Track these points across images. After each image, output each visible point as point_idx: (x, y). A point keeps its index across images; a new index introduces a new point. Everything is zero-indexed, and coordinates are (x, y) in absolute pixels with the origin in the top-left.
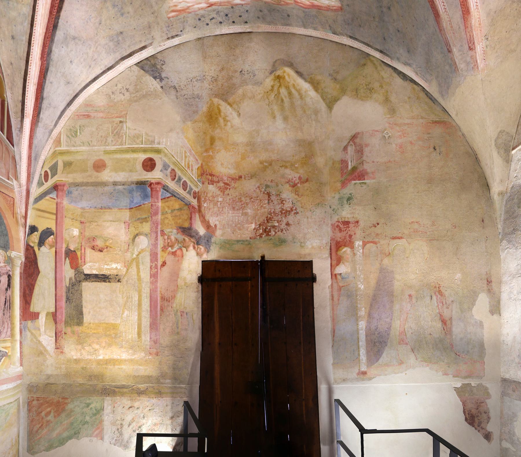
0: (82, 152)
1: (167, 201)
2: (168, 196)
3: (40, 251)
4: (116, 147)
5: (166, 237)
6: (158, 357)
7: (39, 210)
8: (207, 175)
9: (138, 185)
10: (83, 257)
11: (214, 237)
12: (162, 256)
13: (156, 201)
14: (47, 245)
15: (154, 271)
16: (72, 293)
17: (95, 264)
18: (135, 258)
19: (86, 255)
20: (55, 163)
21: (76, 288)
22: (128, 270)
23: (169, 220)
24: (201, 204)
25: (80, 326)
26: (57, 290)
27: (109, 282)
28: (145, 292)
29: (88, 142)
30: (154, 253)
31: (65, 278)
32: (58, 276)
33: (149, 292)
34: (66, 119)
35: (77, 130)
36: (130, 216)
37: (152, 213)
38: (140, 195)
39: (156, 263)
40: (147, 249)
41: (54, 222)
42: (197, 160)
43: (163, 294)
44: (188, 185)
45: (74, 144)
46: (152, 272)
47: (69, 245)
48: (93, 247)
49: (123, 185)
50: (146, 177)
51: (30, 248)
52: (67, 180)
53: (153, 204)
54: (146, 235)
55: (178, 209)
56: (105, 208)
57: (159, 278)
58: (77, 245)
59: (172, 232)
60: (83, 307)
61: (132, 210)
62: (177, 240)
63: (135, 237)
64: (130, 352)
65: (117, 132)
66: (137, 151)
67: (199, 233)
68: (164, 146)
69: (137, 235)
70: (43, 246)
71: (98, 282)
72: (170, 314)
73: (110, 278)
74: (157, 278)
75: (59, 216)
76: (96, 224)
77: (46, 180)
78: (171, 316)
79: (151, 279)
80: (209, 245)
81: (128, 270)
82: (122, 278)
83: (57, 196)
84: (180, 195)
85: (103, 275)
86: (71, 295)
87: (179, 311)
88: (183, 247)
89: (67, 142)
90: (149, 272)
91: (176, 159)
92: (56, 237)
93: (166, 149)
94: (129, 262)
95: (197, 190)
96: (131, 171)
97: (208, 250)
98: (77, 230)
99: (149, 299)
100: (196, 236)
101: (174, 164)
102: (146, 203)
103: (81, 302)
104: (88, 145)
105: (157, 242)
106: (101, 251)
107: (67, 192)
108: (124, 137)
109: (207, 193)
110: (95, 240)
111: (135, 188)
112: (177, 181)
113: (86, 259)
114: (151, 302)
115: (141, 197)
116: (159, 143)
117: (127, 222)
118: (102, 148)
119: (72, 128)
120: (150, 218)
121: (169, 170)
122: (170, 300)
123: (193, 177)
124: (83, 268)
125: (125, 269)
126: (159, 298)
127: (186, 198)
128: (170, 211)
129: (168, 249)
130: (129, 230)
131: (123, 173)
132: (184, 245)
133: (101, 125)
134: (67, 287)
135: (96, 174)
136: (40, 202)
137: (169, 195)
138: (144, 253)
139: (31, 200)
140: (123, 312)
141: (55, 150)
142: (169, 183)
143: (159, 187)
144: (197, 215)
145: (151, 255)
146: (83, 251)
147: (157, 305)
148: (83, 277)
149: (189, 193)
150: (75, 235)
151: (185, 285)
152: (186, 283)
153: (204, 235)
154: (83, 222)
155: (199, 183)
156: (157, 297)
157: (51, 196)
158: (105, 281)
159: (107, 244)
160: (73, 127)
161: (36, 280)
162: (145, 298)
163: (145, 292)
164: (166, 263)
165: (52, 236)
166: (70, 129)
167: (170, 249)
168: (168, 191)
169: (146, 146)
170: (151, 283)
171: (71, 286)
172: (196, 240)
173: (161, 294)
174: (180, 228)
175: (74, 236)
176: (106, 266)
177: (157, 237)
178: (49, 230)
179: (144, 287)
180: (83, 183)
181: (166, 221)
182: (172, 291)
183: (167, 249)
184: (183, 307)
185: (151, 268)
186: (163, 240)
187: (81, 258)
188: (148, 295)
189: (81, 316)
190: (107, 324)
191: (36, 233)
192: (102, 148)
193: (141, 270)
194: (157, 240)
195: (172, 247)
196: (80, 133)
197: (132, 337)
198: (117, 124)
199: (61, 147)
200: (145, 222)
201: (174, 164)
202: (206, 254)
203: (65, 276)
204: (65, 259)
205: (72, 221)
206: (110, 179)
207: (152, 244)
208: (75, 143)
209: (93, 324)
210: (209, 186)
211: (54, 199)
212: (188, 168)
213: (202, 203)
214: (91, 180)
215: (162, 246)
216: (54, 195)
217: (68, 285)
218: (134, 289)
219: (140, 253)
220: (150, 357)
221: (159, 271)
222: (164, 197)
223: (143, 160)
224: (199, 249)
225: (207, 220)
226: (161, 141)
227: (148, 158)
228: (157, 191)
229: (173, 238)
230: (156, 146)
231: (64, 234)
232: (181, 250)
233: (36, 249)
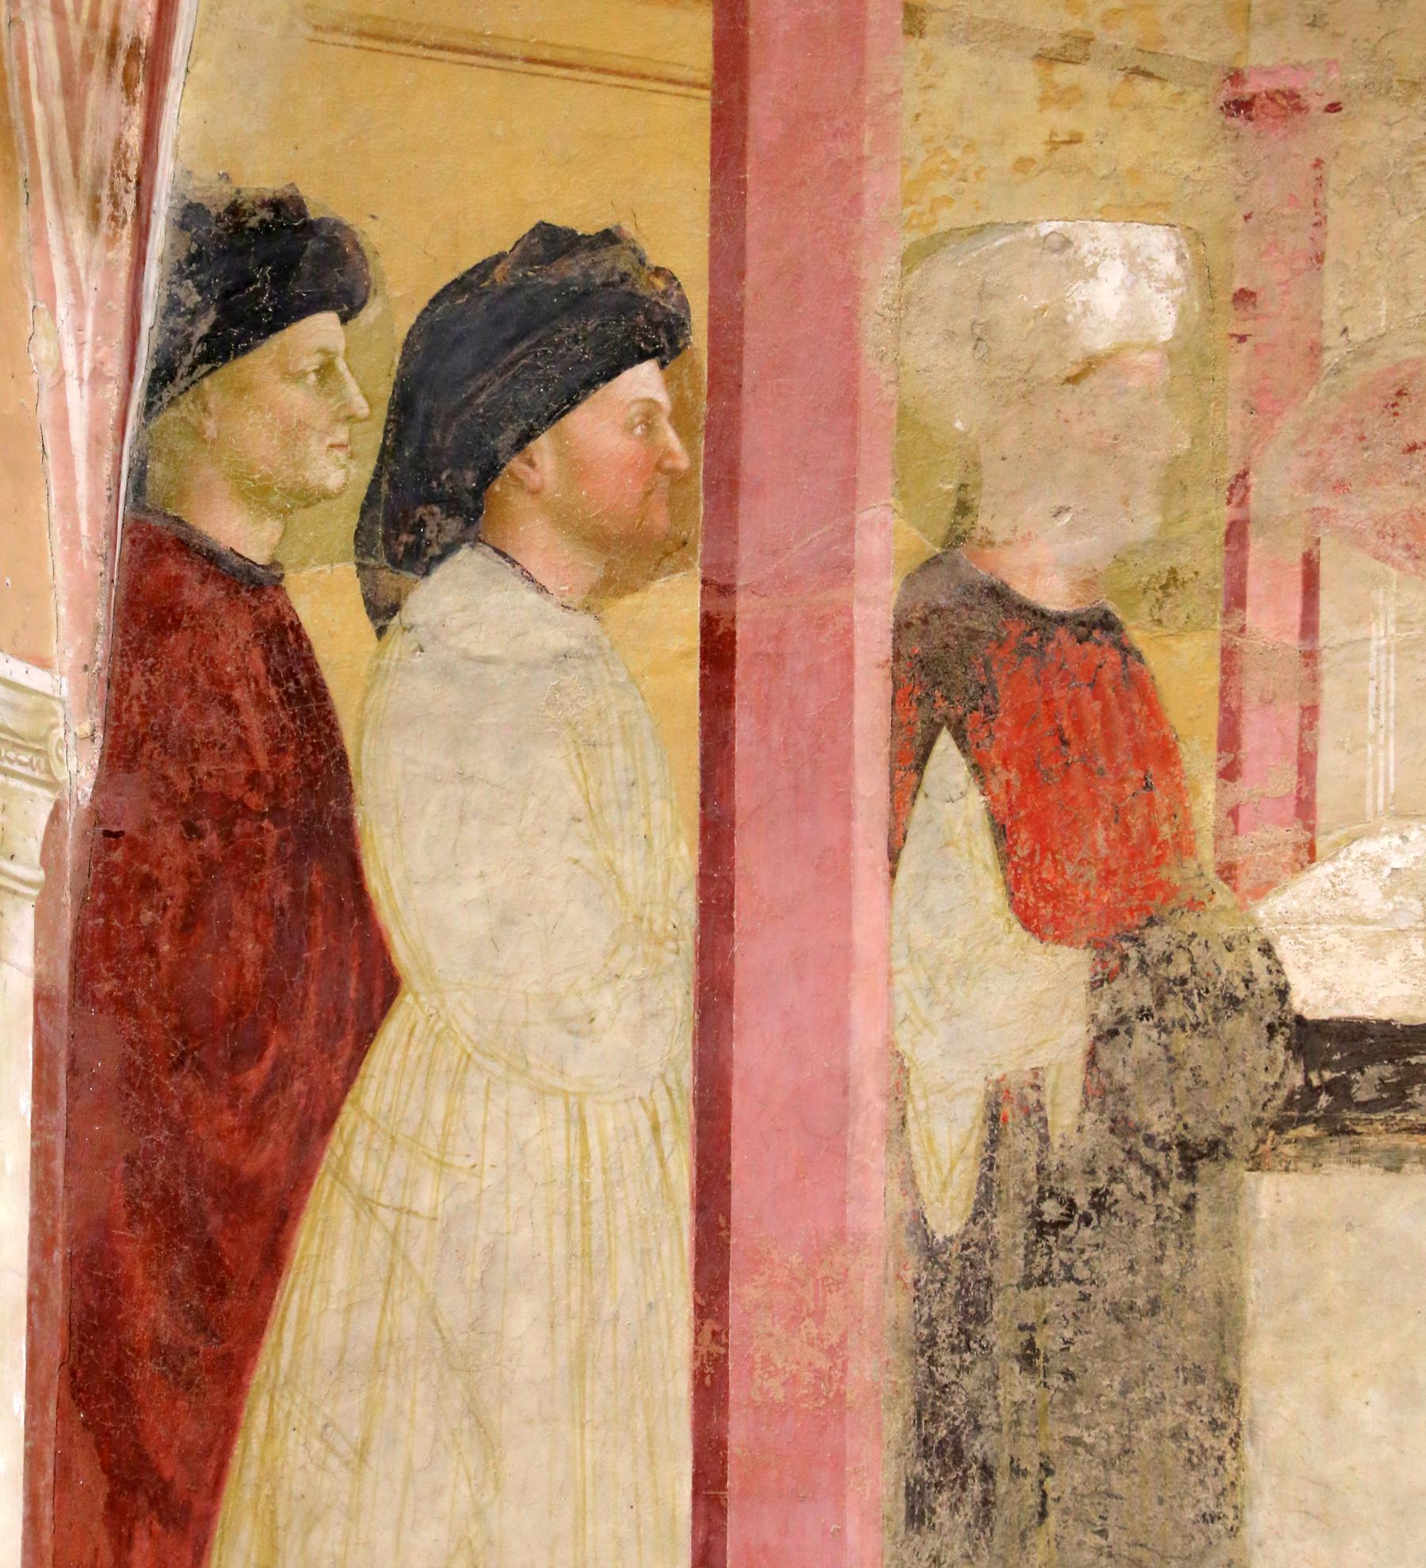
19: (1332, 693)
31: (898, 1093)
113: (1328, 761)
124: (1268, 911)
134: (931, 1252)
187: (1229, 737)
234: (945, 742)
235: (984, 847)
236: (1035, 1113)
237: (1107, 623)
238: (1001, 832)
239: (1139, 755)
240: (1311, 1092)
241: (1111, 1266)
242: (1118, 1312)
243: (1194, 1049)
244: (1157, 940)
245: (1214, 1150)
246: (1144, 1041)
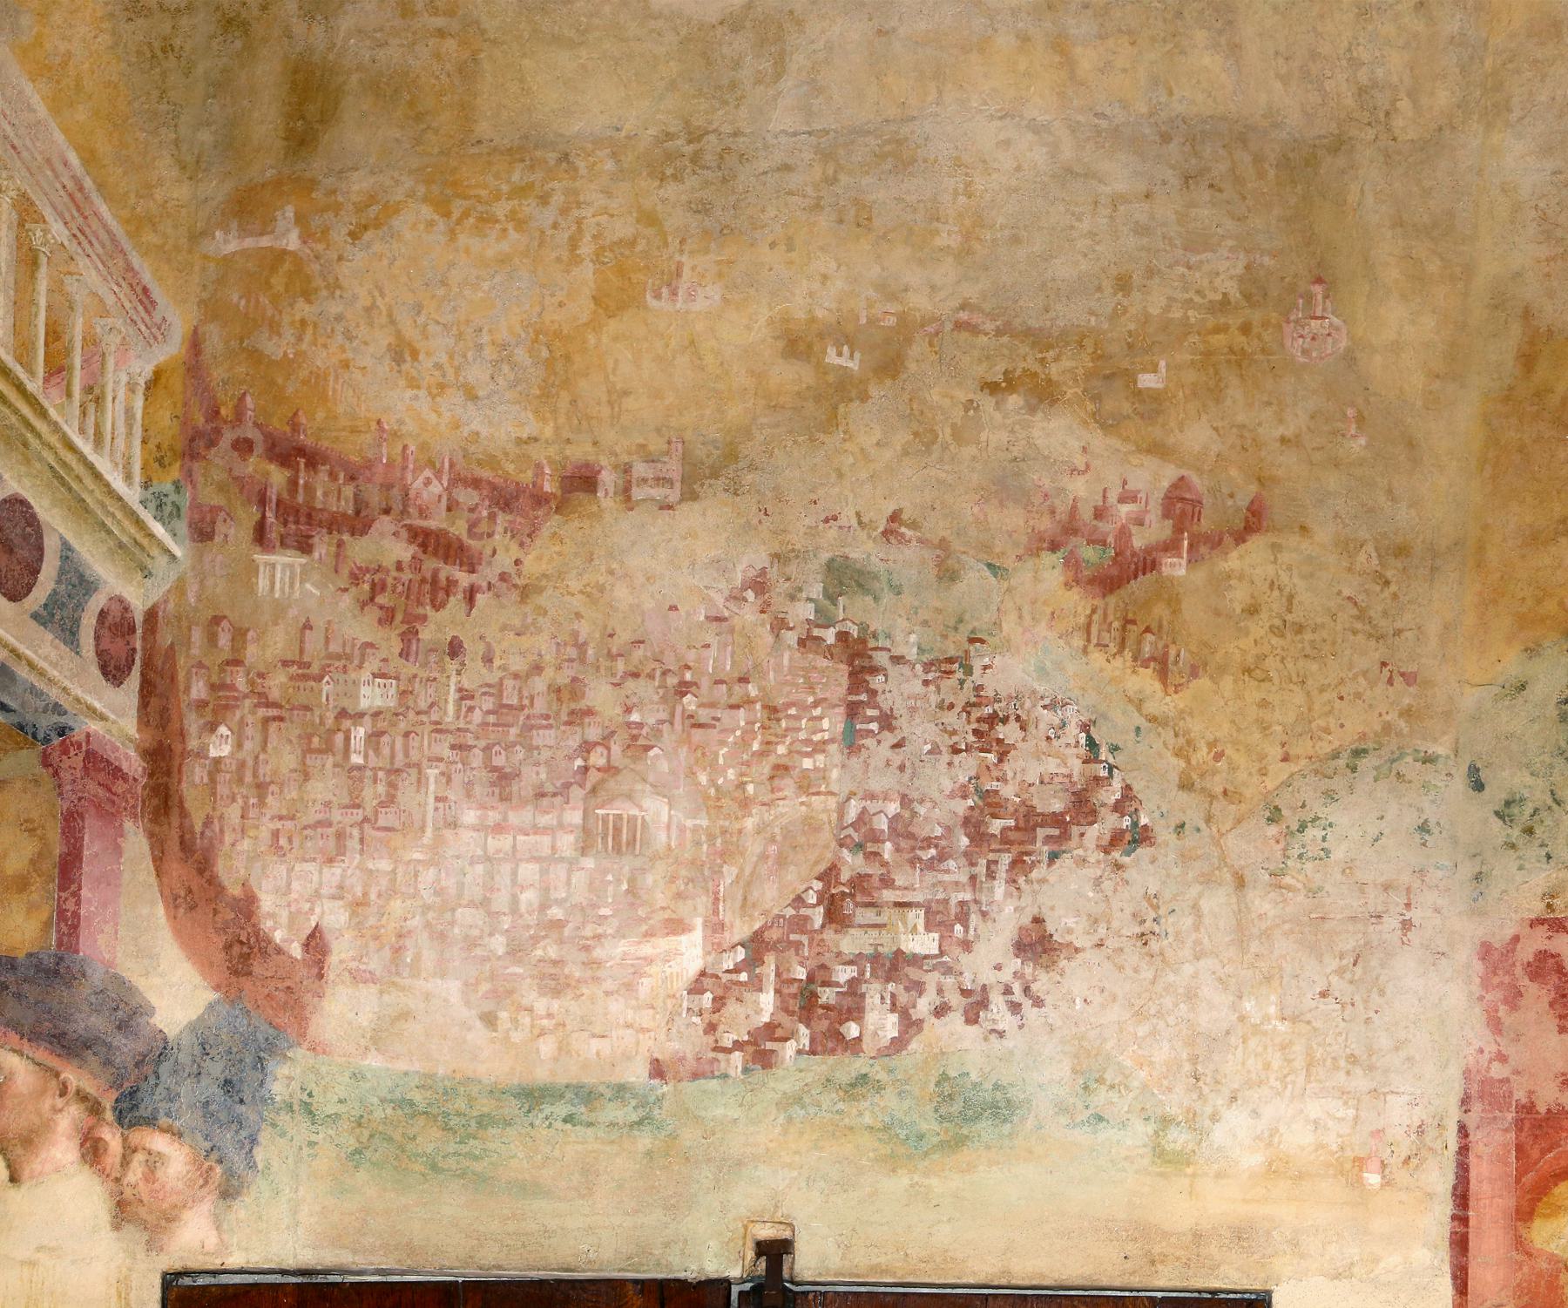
11: (299, 1053)
67: (151, 1011)
80: (240, 1122)
97: (230, 1174)
100: (119, 1040)
153: (192, 1027)
172: (116, 1084)
202: (206, 1207)
224: (139, 1157)
225: (235, 891)
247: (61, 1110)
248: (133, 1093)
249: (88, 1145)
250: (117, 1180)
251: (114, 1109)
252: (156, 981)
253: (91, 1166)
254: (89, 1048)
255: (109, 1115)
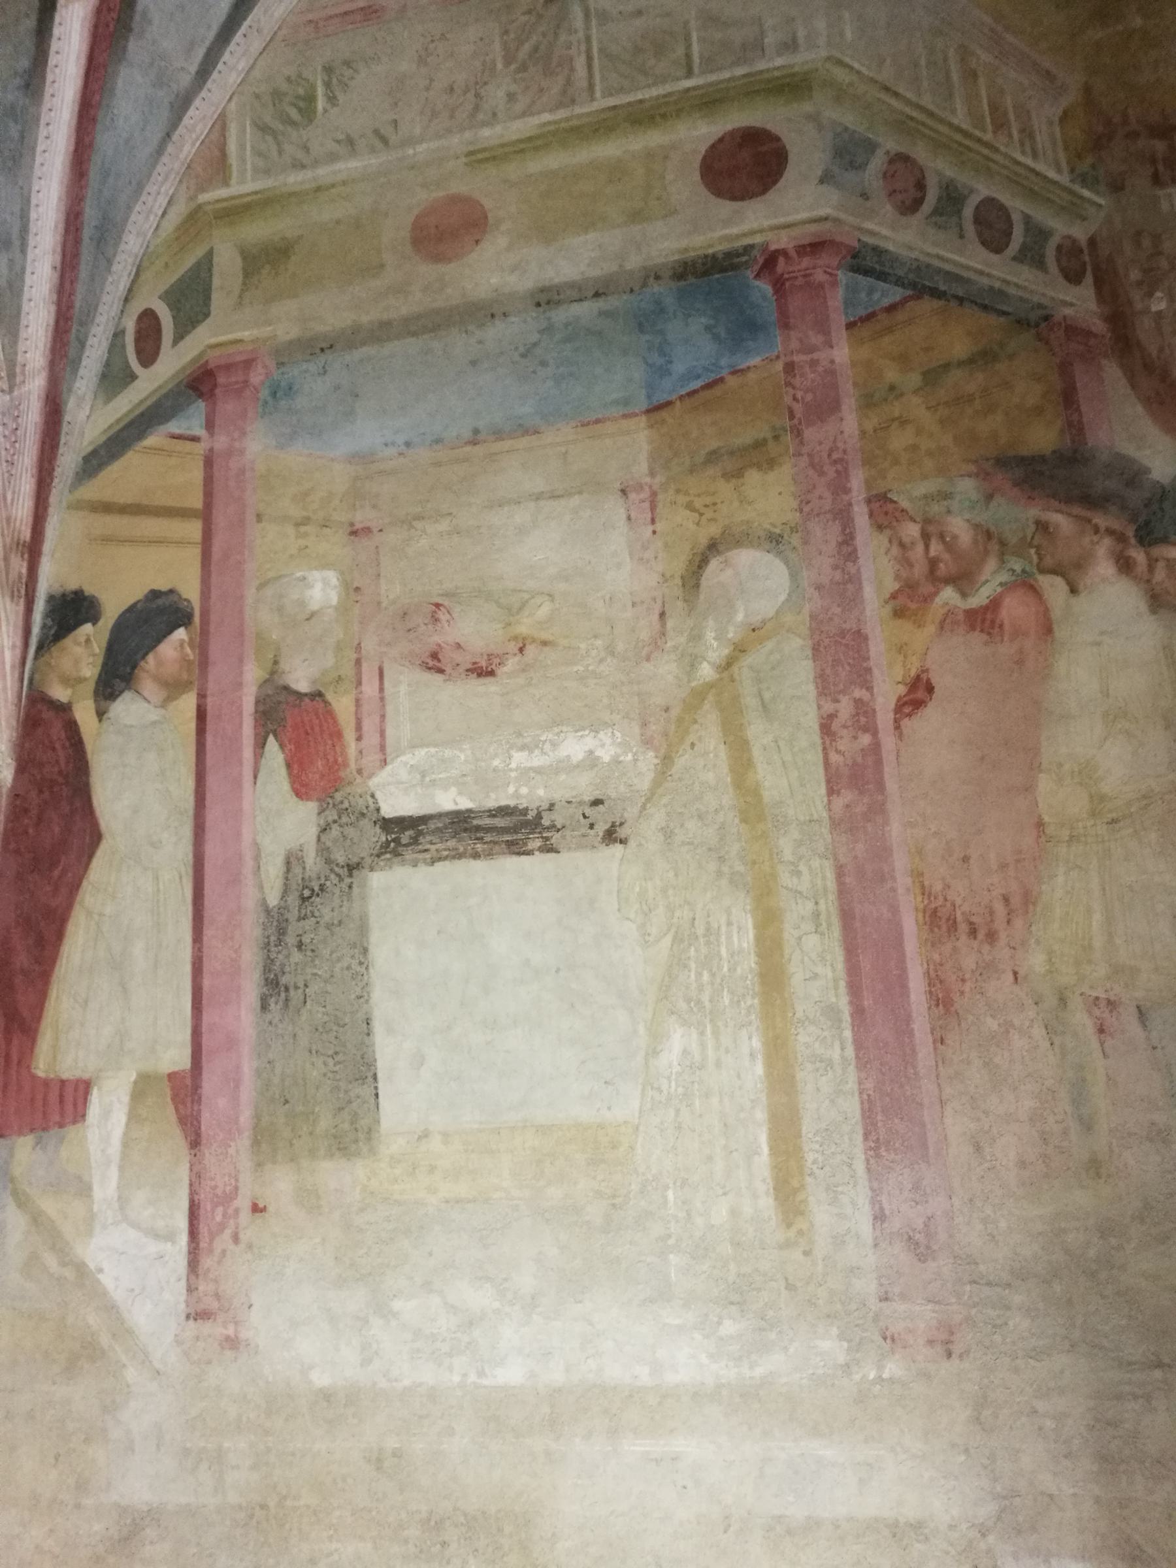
0: (344, 183)
1: (890, 330)
2: (886, 302)
3: (105, 724)
4: (535, 121)
5: (912, 531)
6: (955, 1361)
7: (107, 508)
8: (1133, 135)
9: (692, 280)
10: (369, 725)
12: (901, 649)
13: (815, 339)
14: (148, 686)
15: (850, 745)
16: (300, 946)
17: (448, 753)
18: (711, 686)
19: (389, 709)
20: (198, 264)
21: (327, 915)
22: (667, 760)
23: (919, 432)
24: (1130, 303)
25: (358, 1154)
26: (208, 932)
27: (549, 849)
28: (804, 884)
29: (376, 132)
30: (843, 633)
31: (257, 858)
32: (212, 849)
33: (831, 884)
34: (257, 45)
35: (313, 87)
36: (653, 457)
37: (798, 408)
38: (708, 328)
39: (858, 693)
40: (789, 618)
41: (193, 555)
42: (1049, 75)
43: (938, 887)
44: (1016, 217)
45: (300, 155)
46: (834, 758)
47: (284, 665)
48: (435, 656)
49: (597, 295)
50: (735, 230)
51: (47, 715)
52: (266, 331)
53: (797, 358)
54: (774, 541)
55: (971, 361)
56: (498, 434)
57: (891, 785)
58: (330, 661)
59: (946, 496)
60: (378, 1027)
61: (664, 414)
62: (989, 535)
63: (699, 563)
64: (729, 1328)
65: (536, 49)
66: (664, 116)
67: (1147, 471)
68: (824, 53)
69: (713, 547)
70: (127, 696)
71: (476, 856)
72: (1008, 1027)
73: (552, 827)
74: (881, 787)
75: (220, 520)
76: (444, 526)
77: (148, 355)
78: (1018, 1042)
79: (839, 803)
81: (667, 760)
82: (631, 813)
83: (210, 425)
84: (968, 281)
85: (503, 811)
86: (296, 956)
87: (1076, 1002)
88: (1042, 571)
89: (259, 154)
90: (816, 757)
91: (908, 102)
92: (205, 632)
93: (840, 63)
94: (675, 712)
95: (1080, 233)
96: (636, 216)
98: (332, 577)
99: (837, 932)
101: (903, 126)
102: (755, 361)
103: (363, 997)
104: (378, 144)
105: (853, 571)
106: (483, 671)
107: (264, 393)
108: (580, 63)
109: (1157, 238)
110: (443, 616)
111: (669, 301)
112: (936, 212)
113: (390, 732)
114: (850, 951)
115: (716, 338)
116: (790, 45)
117: (640, 487)
118: (456, 142)
119: (284, 87)
120: (788, 438)
121: (877, 163)
122: (1000, 924)
123: (1040, 167)
124: (373, 783)
125: (649, 761)
126: (910, 925)
127: (1012, 291)
128: (915, 379)
129: (939, 600)
130: (659, 526)
131: (591, 236)
132: (1049, 561)
133: (443, 37)
134: (268, 911)
135: (427, 271)
136: (114, 469)
137: (896, 294)
138: (770, 645)
139: (68, 461)
140: (657, 1038)
141: (193, 205)
142: (885, 232)
143: (820, 268)
144: (1112, 371)
145: (816, 649)
146: (370, 688)
147: (903, 970)
148: (375, 836)
149: (1031, 255)
150: (314, 606)
151: (1093, 814)
152: (1098, 801)
154: (367, 530)
155: (1086, 193)
156: (895, 909)
157: (174, 427)
158: (517, 848)
159: (523, 629)
160: (289, 79)
161: (75, 887)
162: (808, 926)
163: (804, 884)
164: (930, 689)
165: (181, 634)
166: (277, 95)
167: (948, 594)
168: (882, 276)
169: (713, 78)
170: (835, 824)
171: (293, 900)
172: (1133, 519)
173: (925, 891)
174: (1002, 462)
175: (313, 615)
176: (519, 758)
177: (848, 539)
178: (160, 602)
179: (788, 855)
180: (356, 329)
181: (899, 440)
182: (1003, 866)
183: (928, 599)
184: (1102, 971)
185: (826, 728)
186: (895, 550)
187: (359, 727)
188: (829, 905)
189: (366, 1091)
190: (543, 1130)
191: (87, 628)
192: (456, 142)
193: (756, 752)
194: (852, 556)
195: (963, 580)
196: (332, 99)
197: (734, 1213)
198: (529, 12)
199: (226, 183)
200: (759, 466)
201: (903, 126)
203: (257, 847)
204: (260, 744)
205: (300, 536)
206: (512, 279)
207: (819, 588)
208: (306, 149)
209: (446, 1136)
210: (1160, 193)
211: (195, 439)
212: (1000, 125)
213: (1136, 296)
214: (401, 308)
215: (891, 585)
216: (192, 421)
217: (273, 900)
218: (719, 874)
219: (740, 649)
220: (893, 1368)
221: (888, 742)
222: (862, 312)
223: (703, 149)
224: (1161, 565)
226: (801, 33)
227: (732, 134)
228: (817, 291)
229: (959, 527)
230: (774, 63)
231: (248, 612)
232: (1034, 590)
233: (84, 713)
234: (271, 738)
235: (283, 771)
236: (301, 860)
237: (320, 694)
238: (289, 766)
239: (331, 736)
240: (388, 843)
241: (326, 911)
242: (329, 926)
243: (350, 832)
244: (338, 796)
245: (358, 866)
246: (335, 831)
247: (1098, 543)
248: (1147, 523)
249: (1121, 561)
250: (1148, 581)
251: (1136, 536)
252: (1148, 452)
253: (1127, 575)
254: (1108, 501)
255: (1133, 541)
